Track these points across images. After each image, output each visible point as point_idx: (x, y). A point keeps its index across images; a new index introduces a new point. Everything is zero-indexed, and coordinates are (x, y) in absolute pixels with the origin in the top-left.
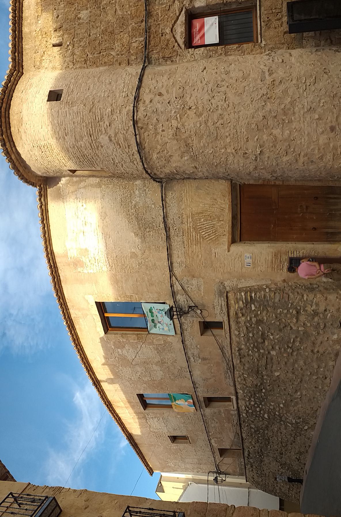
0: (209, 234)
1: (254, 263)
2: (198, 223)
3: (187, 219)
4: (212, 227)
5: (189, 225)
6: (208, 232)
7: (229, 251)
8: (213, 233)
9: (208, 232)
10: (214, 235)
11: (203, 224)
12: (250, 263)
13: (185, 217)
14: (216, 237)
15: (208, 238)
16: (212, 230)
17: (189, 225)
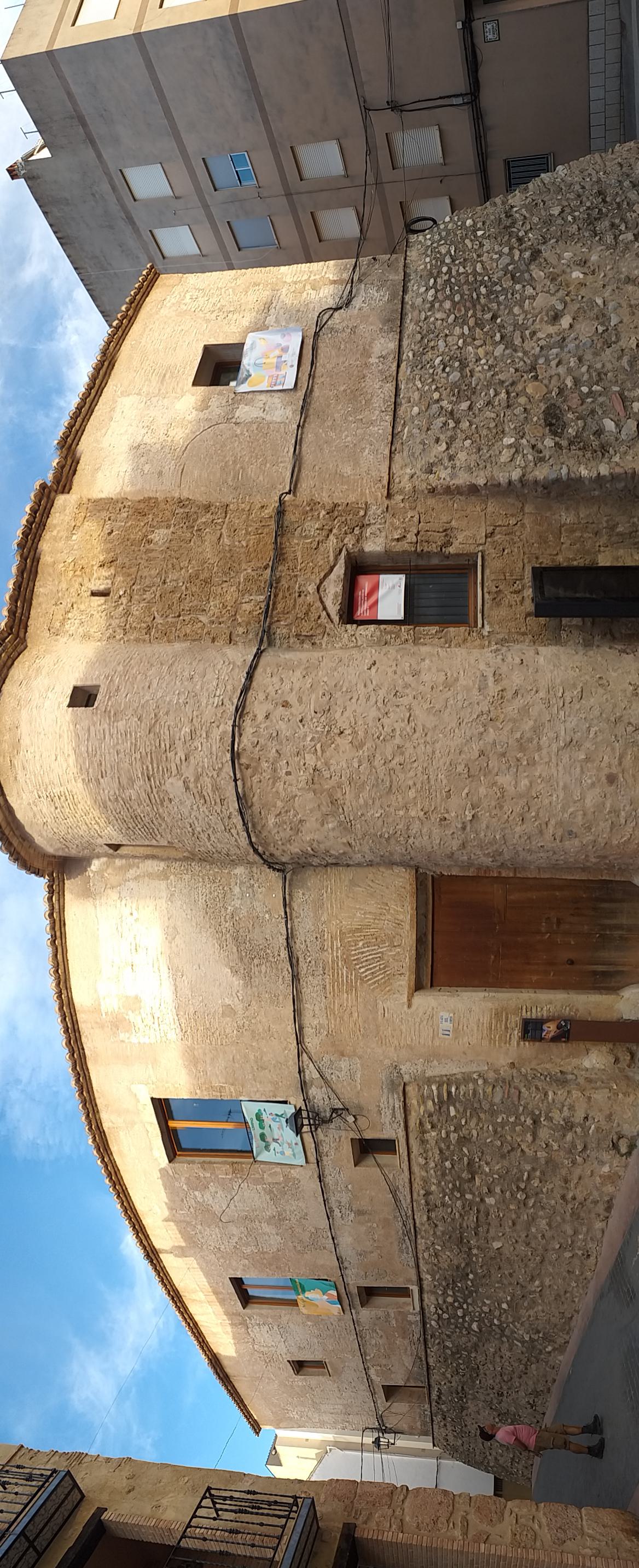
1: (456, 1030)
3: (332, 943)
6: (371, 969)
7: (409, 1006)
8: (380, 969)
9: (371, 969)
11: (363, 953)
15: (369, 980)
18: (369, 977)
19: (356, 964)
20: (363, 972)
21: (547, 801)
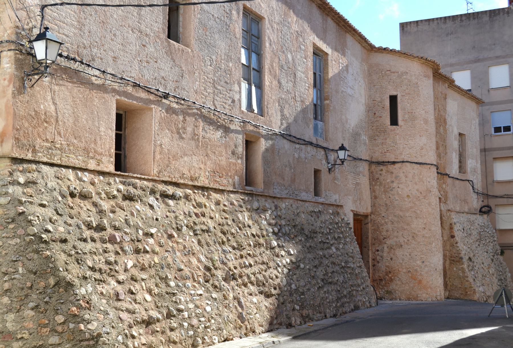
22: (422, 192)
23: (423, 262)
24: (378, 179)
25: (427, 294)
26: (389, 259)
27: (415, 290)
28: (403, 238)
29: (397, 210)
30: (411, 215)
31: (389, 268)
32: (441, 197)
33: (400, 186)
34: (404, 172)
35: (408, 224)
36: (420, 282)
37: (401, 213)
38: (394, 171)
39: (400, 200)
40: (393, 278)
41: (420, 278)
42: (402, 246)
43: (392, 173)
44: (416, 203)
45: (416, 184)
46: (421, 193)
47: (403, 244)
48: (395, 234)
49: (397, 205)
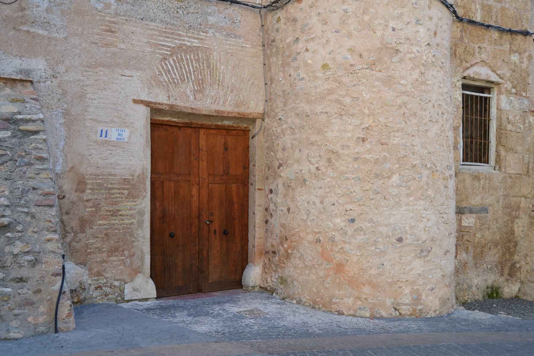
0: (170, 71)
1: (106, 142)
2: (190, 56)
3: (198, 39)
4: (183, 79)
5: (186, 39)
6: (173, 70)
7: (135, 101)
8: (173, 79)
9: (173, 70)
10: (169, 80)
11: (188, 64)
12: (106, 136)
13: (201, 35)
14: (164, 84)
15: (162, 67)
16: (179, 78)
17: (186, 39)
18: (165, 67)
19: (177, 57)
20: (169, 62)
21: (383, 204)
22: (365, 54)
23: (353, 221)
24: (273, 41)
25: (359, 298)
26: (285, 209)
27: (328, 286)
28: (308, 163)
29: (302, 101)
30: (328, 109)
31: (285, 229)
32: (500, 81)
33: (311, 46)
34: (319, 14)
35: (319, 132)
36: (340, 268)
37: (307, 108)
38: (299, 16)
39: (308, 79)
40: (290, 251)
41: (339, 257)
42: (305, 181)
43: (295, 20)
44: (344, 79)
45: (350, 35)
46: (361, 56)
47: (307, 177)
48: (297, 155)
49: (302, 89)
